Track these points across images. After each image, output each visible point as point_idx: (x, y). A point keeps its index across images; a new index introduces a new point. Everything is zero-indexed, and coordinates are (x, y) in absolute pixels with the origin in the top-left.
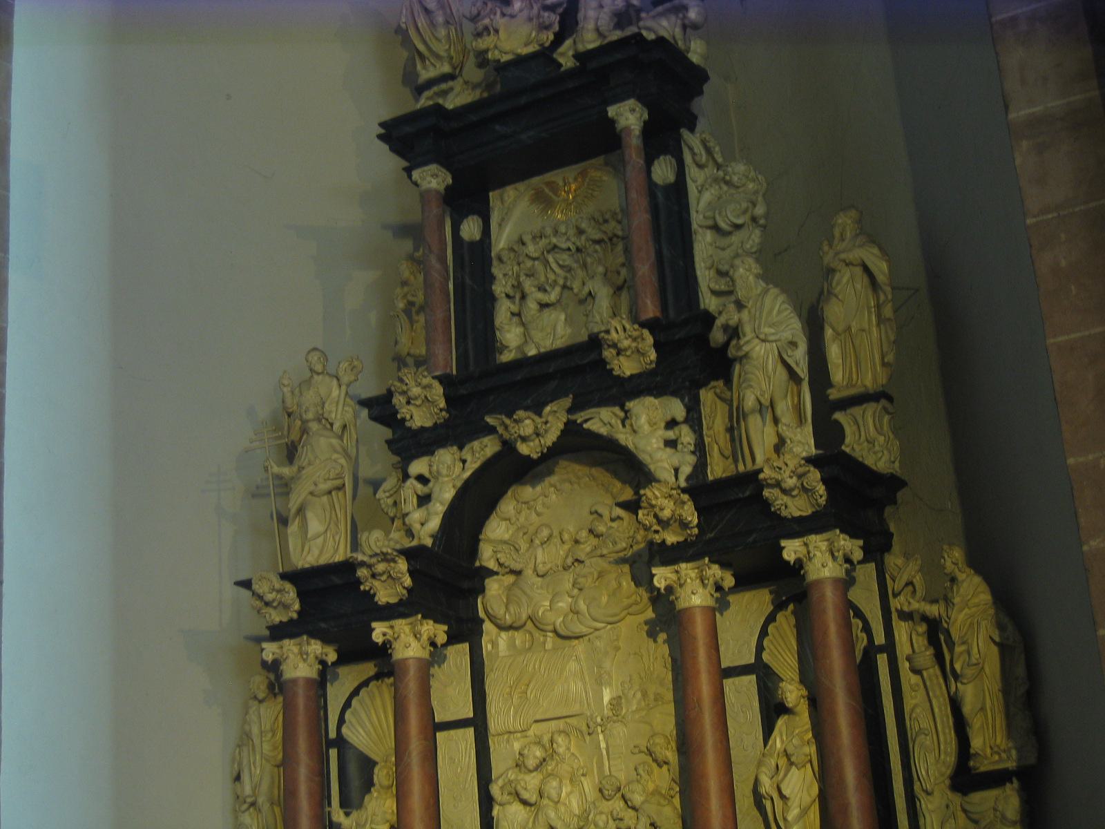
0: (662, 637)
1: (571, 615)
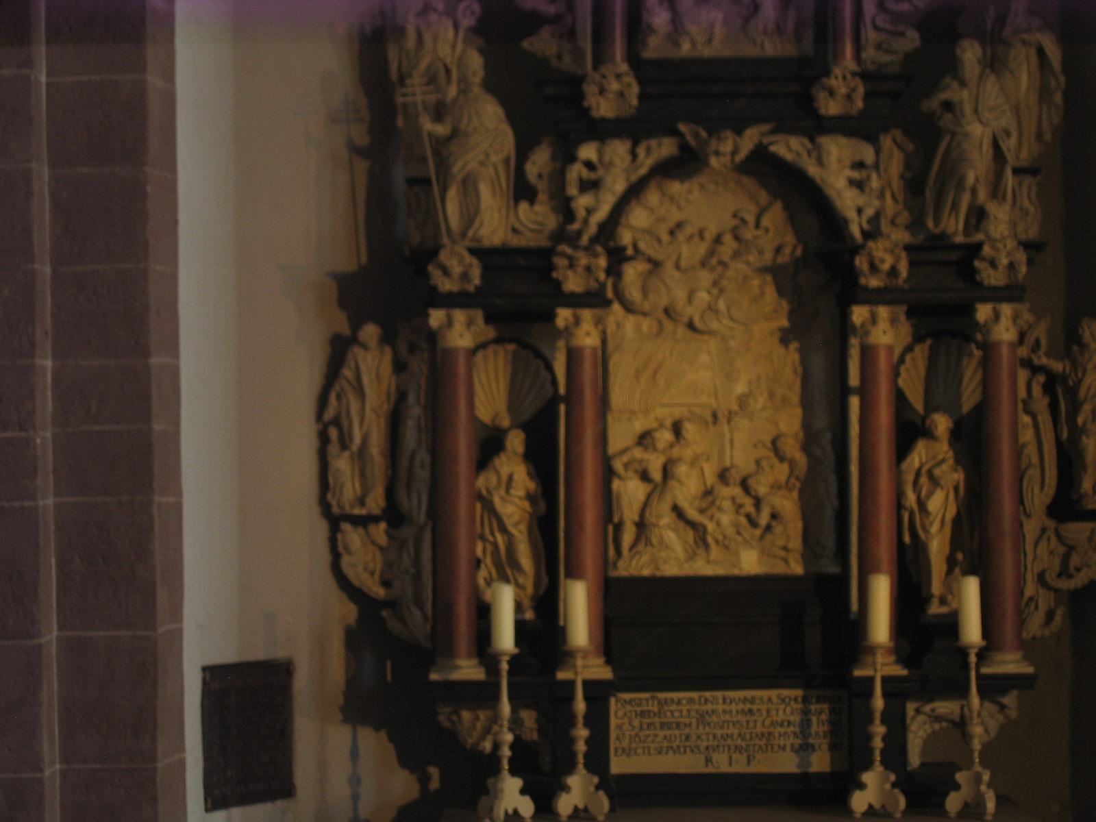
0: (794, 345)
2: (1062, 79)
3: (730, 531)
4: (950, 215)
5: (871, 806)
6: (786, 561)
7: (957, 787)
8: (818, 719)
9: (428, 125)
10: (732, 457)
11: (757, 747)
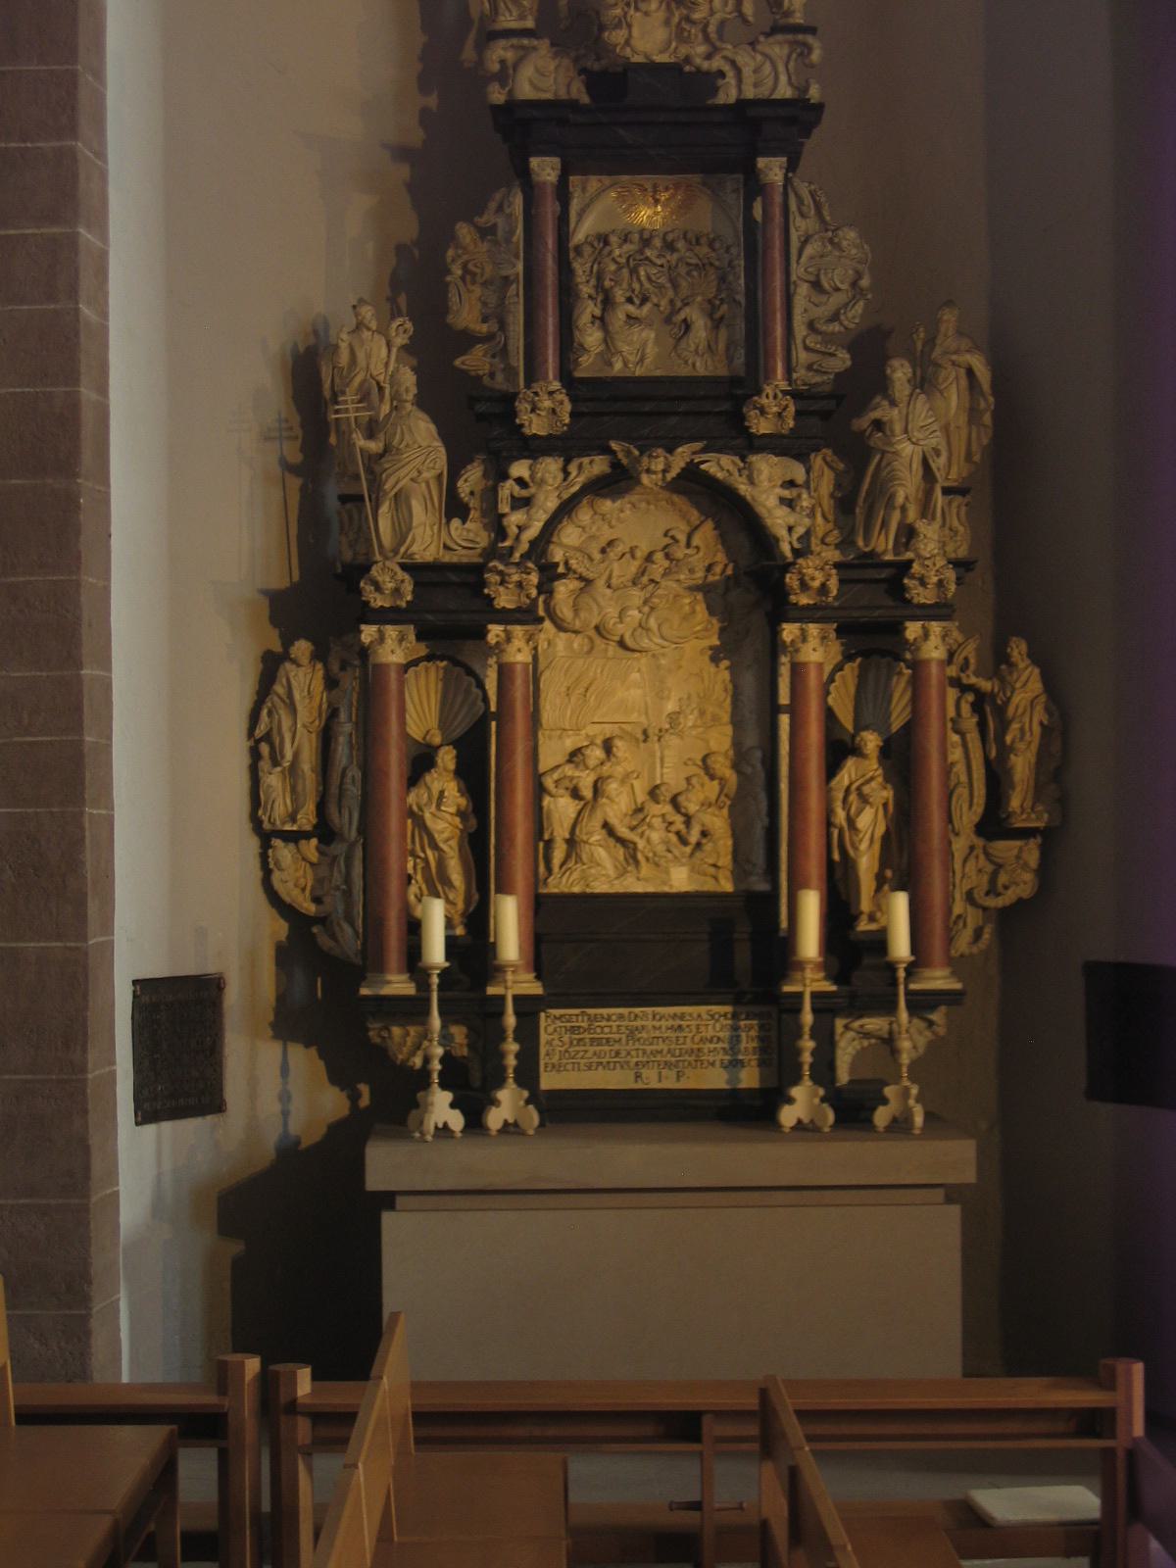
0: (725, 663)
1: (640, 630)
2: (991, 399)
3: (660, 849)
4: (880, 534)
5: (799, 1122)
6: (716, 879)
7: (884, 1101)
8: (747, 1036)
9: (360, 441)
10: (662, 775)
11: (686, 1063)
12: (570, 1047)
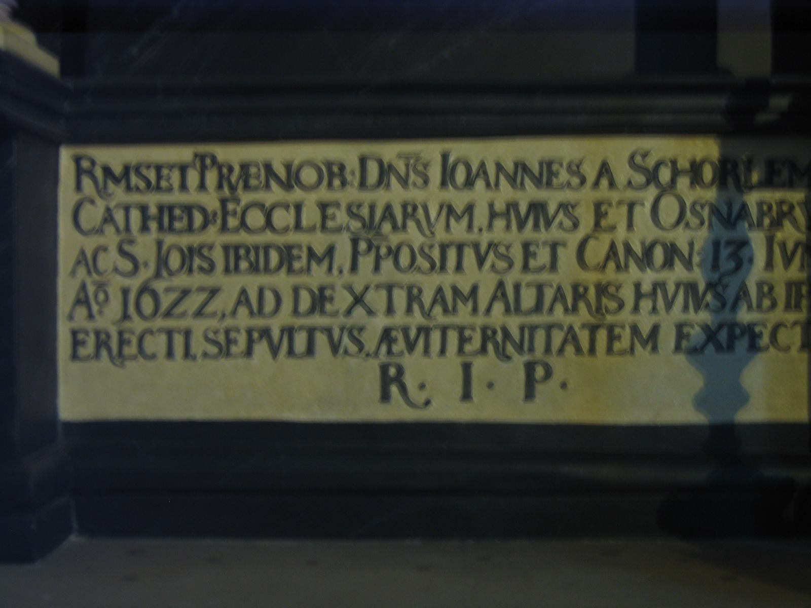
8: (770, 241)
11: (558, 337)
12: (158, 275)
